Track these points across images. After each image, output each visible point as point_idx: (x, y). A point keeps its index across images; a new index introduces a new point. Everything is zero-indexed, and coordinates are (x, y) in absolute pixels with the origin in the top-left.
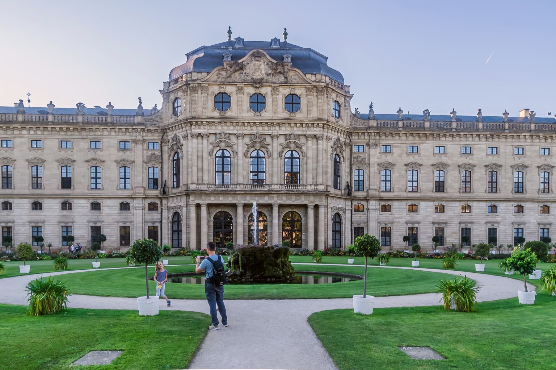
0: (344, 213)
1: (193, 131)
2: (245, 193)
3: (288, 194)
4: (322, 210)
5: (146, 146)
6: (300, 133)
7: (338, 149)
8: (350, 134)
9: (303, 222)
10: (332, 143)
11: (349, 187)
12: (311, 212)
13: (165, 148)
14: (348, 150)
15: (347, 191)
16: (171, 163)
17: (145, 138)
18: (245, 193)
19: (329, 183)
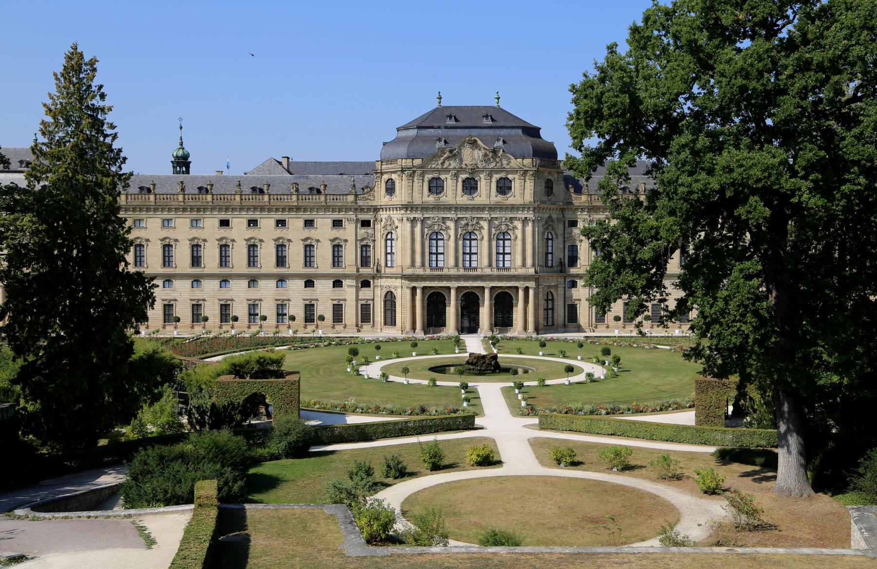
0: (557, 290)
1: (409, 216)
2: (458, 278)
3: (500, 278)
4: (531, 292)
5: (359, 225)
6: (512, 216)
7: (550, 228)
8: (563, 210)
9: (514, 302)
10: (543, 222)
11: (561, 264)
12: (521, 293)
13: (378, 226)
14: (561, 226)
15: (559, 268)
16: (383, 242)
17: (359, 216)
18: (458, 278)
19: (540, 263)
